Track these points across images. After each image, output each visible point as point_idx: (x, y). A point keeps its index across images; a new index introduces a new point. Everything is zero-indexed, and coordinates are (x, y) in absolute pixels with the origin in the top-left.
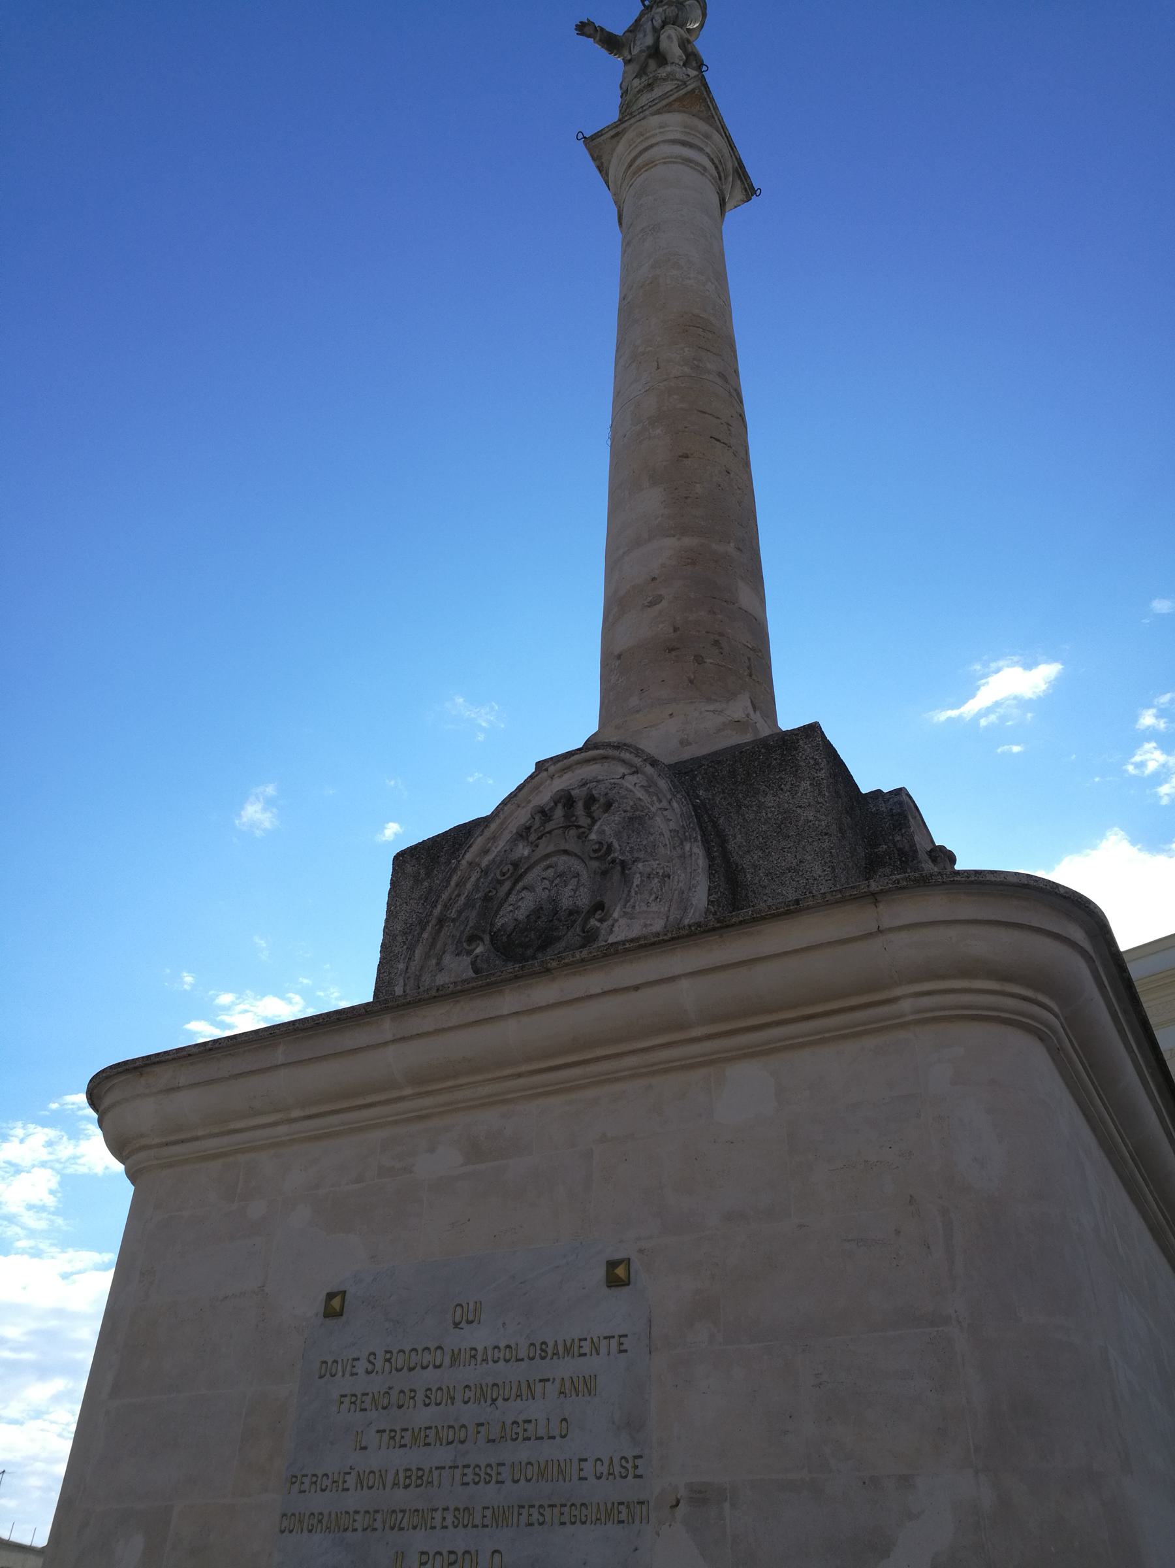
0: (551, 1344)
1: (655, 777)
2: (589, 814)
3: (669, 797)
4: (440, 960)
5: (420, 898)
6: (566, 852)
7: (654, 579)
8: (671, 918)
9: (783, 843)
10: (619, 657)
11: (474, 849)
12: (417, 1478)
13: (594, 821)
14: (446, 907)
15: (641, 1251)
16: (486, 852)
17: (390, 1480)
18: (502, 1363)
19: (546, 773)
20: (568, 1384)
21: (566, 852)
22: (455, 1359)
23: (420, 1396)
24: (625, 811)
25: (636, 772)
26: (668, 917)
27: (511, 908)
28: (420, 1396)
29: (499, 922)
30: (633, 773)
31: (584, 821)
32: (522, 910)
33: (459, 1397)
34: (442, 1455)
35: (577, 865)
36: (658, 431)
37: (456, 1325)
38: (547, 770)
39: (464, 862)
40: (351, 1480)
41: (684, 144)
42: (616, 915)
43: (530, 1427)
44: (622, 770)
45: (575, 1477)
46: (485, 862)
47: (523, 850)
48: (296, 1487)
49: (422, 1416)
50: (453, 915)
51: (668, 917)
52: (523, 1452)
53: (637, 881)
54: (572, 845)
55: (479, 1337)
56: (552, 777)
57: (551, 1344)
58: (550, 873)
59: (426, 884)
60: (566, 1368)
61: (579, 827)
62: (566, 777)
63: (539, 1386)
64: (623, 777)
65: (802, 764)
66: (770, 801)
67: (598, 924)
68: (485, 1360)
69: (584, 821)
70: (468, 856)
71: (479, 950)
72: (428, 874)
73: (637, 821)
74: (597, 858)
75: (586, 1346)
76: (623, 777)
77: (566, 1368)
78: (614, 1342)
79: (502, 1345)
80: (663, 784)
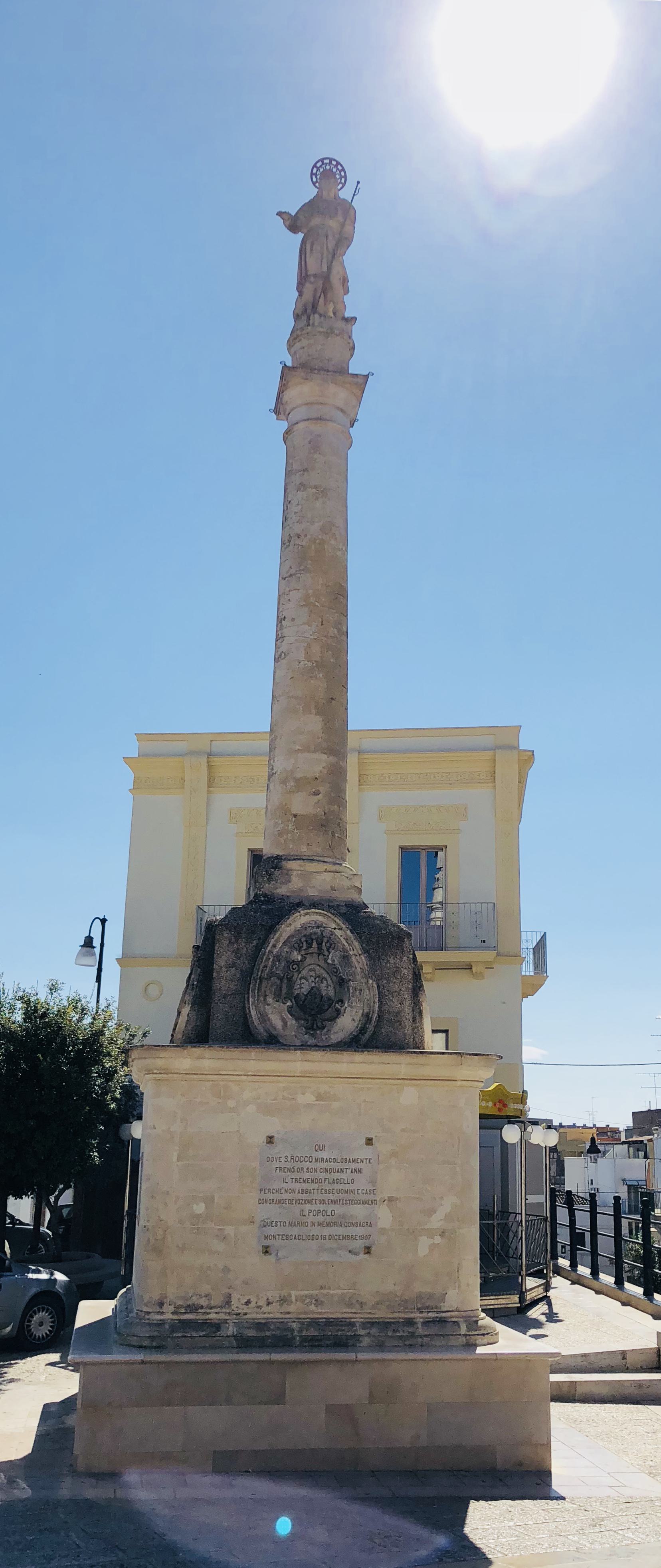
0: (348, 1159)
1: (352, 938)
2: (328, 950)
3: (360, 953)
4: (265, 1000)
5: (233, 952)
6: (319, 965)
7: (316, 778)
8: (365, 1011)
9: (395, 980)
10: (295, 816)
11: (271, 945)
12: (306, 1191)
13: (329, 953)
14: (262, 971)
15: (376, 1136)
16: (274, 946)
17: (297, 1191)
18: (332, 1163)
19: (299, 914)
20: (353, 1170)
21: (319, 965)
22: (316, 1160)
23: (305, 1170)
24: (341, 951)
25: (340, 929)
26: (364, 1010)
27: (298, 986)
28: (305, 1170)
29: (296, 992)
30: (339, 929)
31: (326, 953)
32: (304, 989)
33: (318, 1170)
34: (316, 1186)
35: (325, 975)
36: (321, 675)
37: (316, 1151)
38: (299, 912)
39: (267, 951)
40: (283, 1191)
41: (342, 411)
42: (346, 1005)
43: (342, 1180)
44: (334, 926)
45: (356, 1193)
46: (275, 951)
48: (263, 1192)
49: (306, 1176)
50: (266, 976)
51: (364, 1010)
52: (340, 1187)
53: (351, 991)
54: (322, 963)
55: (324, 1155)
56: (300, 916)
57: (348, 1159)
58: (313, 973)
59: (235, 945)
60: (353, 1166)
61: (324, 955)
62: (307, 916)
63: (345, 1170)
64: (335, 929)
65: (405, 949)
66: (392, 961)
67: (339, 1007)
68: (327, 1161)
69: (326, 953)
70: (269, 948)
71: (289, 1003)
72: (237, 941)
73: (346, 958)
74: (335, 976)
75: (359, 1161)
76: (335, 929)
77: (353, 1166)
78: (368, 1160)
79: (332, 1158)
80: (356, 944)
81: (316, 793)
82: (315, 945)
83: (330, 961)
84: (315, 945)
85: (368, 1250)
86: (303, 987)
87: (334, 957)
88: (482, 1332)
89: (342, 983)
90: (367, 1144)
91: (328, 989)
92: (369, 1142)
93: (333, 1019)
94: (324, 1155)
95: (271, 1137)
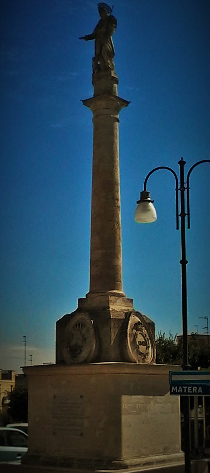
41: (107, 109)
47: (73, 332)
81: (97, 266)
82: (78, 327)
83: (82, 332)
84: (78, 327)
85: (81, 434)
86: (73, 343)
87: (84, 331)
88: (112, 465)
89: (85, 339)
90: (81, 397)
91: (80, 343)
92: (81, 397)
93: (80, 353)
94: (68, 401)
95: (54, 396)
